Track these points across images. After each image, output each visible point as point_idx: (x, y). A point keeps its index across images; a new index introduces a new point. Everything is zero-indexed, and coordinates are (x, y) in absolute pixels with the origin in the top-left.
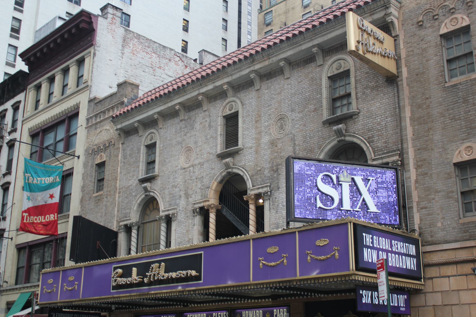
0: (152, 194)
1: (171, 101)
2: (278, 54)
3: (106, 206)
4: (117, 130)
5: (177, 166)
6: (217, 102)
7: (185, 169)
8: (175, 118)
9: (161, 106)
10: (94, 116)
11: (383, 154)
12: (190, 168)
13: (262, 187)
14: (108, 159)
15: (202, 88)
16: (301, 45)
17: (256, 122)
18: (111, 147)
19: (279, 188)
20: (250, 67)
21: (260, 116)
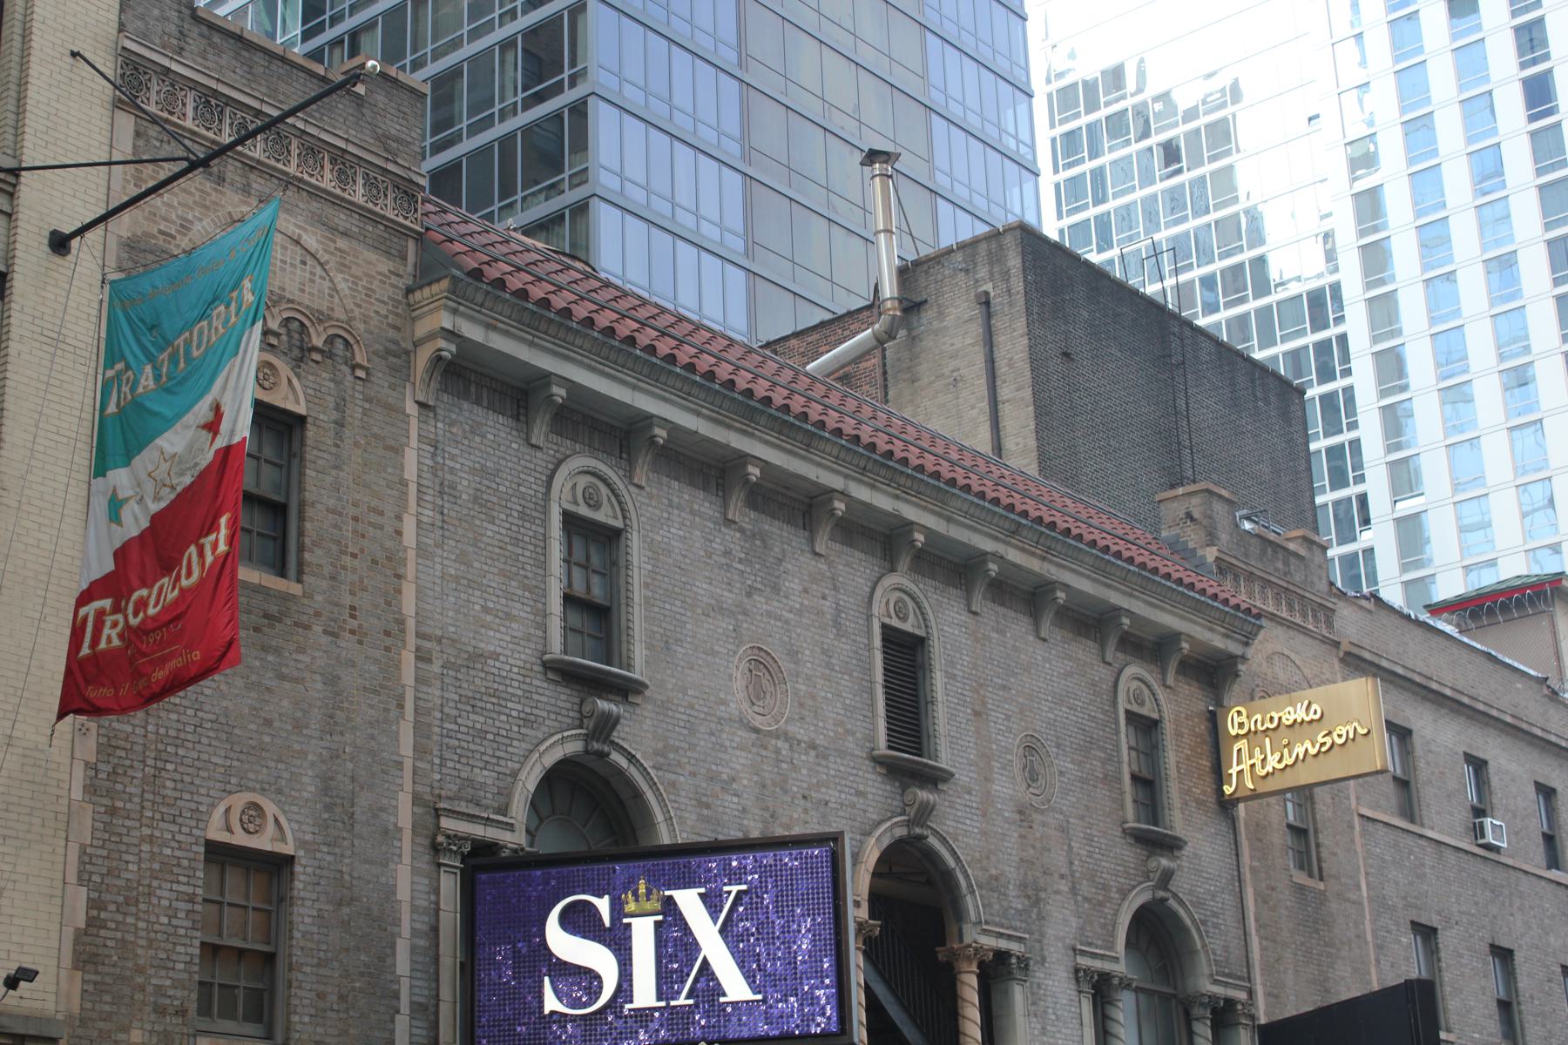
0: (624, 763)
1: (744, 432)
2: (1063, 567)
3: (332, 681)
4: (451, 335)
5: (724, 702)
6: (858, 554)
7: (756, 730)
8: (701, 494)
9: (698, 414)
10: (194, 85)
11: (1225, 975)
12: (780, 744)
13: (1009, 937)
14: (326, 417)
15: (860, 481)
16: (1109, 586)
17: (977, 714)
18: (347, 370)
19: (1043, 960)
20: (996, 539)
21: (984, 703)
